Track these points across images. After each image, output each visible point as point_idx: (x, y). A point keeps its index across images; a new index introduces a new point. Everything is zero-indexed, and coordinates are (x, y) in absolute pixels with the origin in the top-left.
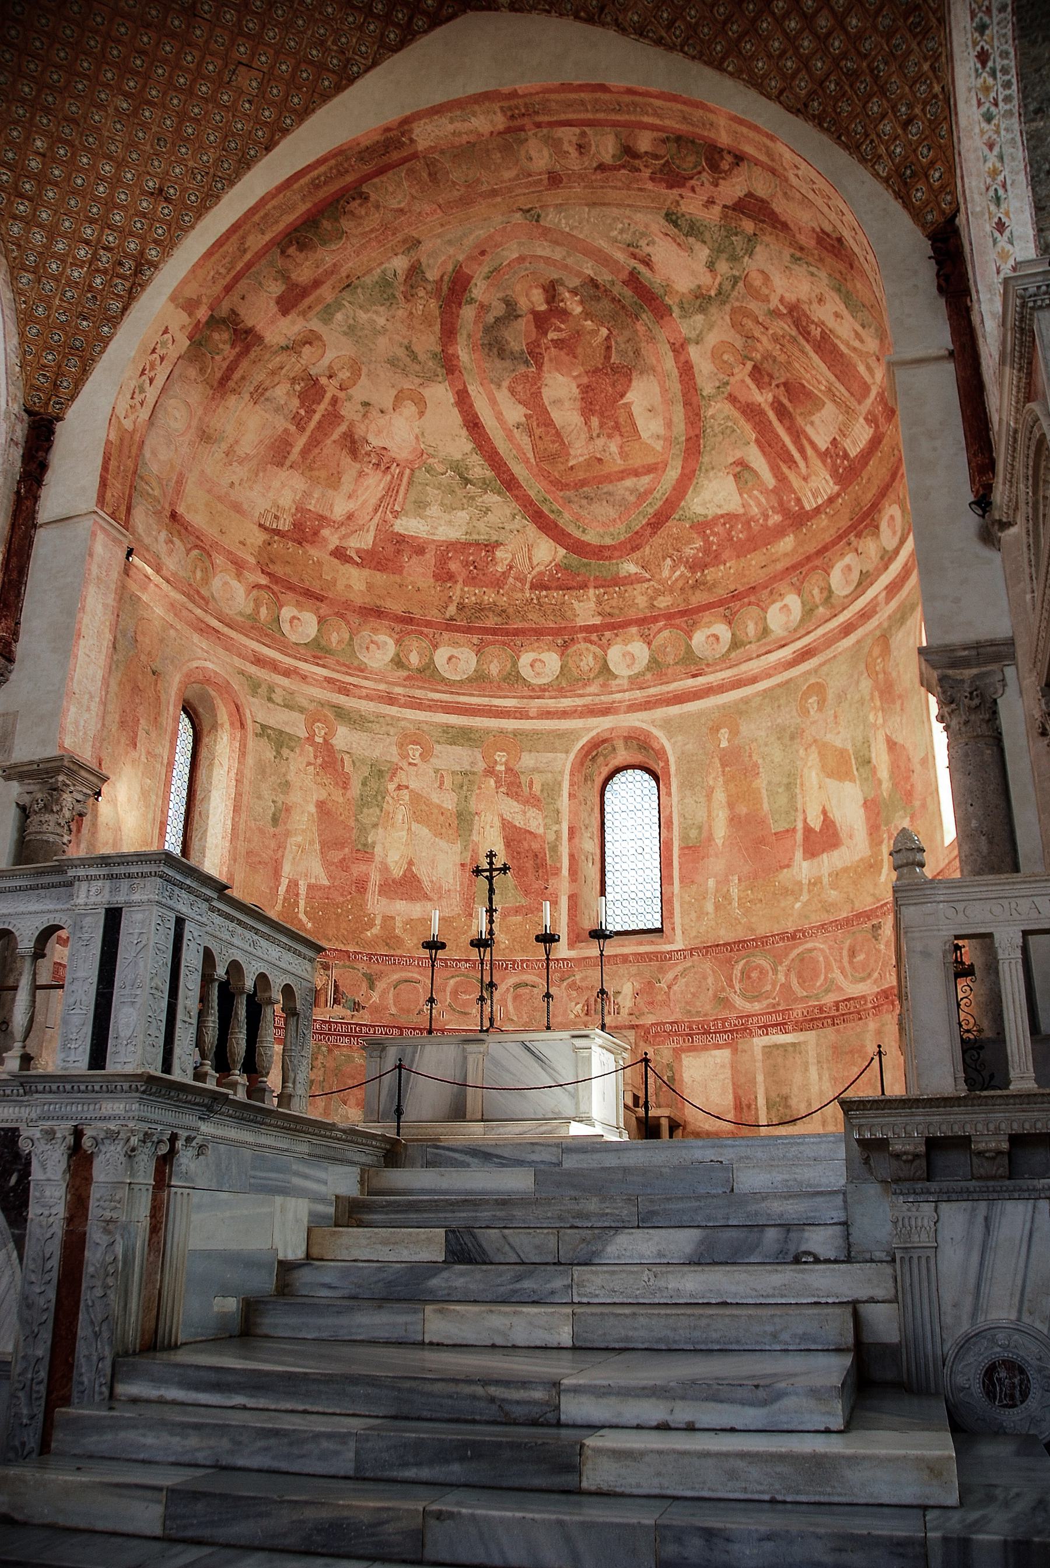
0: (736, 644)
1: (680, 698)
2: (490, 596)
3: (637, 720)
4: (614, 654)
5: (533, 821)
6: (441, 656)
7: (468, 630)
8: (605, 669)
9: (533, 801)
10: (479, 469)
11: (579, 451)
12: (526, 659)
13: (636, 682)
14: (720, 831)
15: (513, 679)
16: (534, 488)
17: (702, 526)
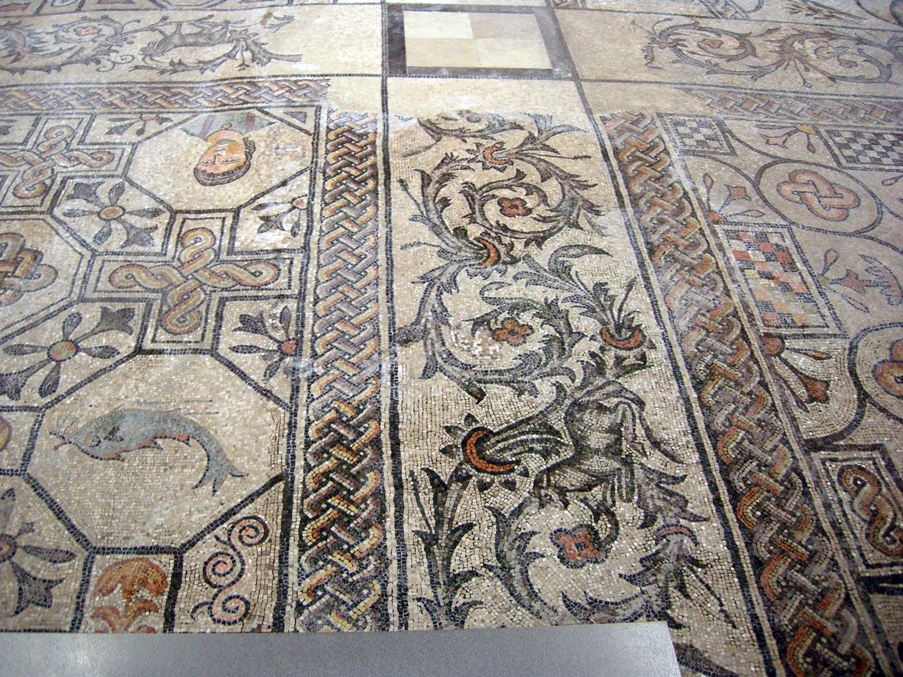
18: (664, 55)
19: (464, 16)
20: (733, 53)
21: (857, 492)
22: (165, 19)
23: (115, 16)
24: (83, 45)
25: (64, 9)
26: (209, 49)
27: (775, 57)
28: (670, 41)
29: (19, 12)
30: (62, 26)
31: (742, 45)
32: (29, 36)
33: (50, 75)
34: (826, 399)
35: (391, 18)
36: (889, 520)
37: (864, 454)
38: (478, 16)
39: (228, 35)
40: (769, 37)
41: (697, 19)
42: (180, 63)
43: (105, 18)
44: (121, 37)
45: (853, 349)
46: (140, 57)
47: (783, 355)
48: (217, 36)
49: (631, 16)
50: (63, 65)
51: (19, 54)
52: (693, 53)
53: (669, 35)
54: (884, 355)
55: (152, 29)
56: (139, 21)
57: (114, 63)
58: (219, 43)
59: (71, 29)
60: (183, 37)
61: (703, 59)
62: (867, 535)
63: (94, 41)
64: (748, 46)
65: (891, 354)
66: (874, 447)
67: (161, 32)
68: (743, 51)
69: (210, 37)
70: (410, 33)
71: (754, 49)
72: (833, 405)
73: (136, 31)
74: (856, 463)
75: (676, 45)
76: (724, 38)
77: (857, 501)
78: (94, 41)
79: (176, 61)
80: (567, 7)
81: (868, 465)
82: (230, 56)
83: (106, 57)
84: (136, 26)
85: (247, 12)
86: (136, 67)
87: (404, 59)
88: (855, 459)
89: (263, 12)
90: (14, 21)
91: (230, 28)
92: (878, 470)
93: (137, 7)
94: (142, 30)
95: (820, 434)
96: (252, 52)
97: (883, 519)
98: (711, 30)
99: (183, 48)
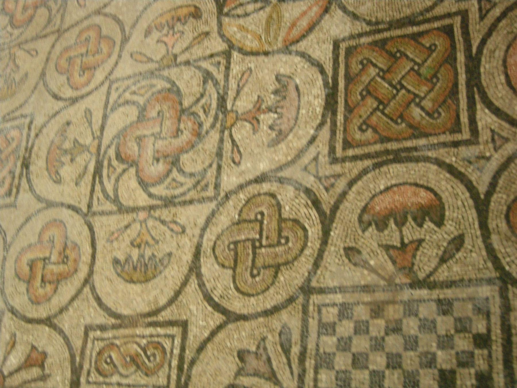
21: (115, 366)
34: (45, 355)
36: (139, 350)
37: (89, 345)
45: (13, 311)
47: (6, 373)
54: (22, 287)
62: (147, 375)
65: (24, 281)
66: (86, 334)
72: (50, 350)
74: (94, 354)
77: (121, 370)
81: (98, 345)
88: (91, 355)
92: (103, 339)
95: (68, 374)
97: (138, 355)
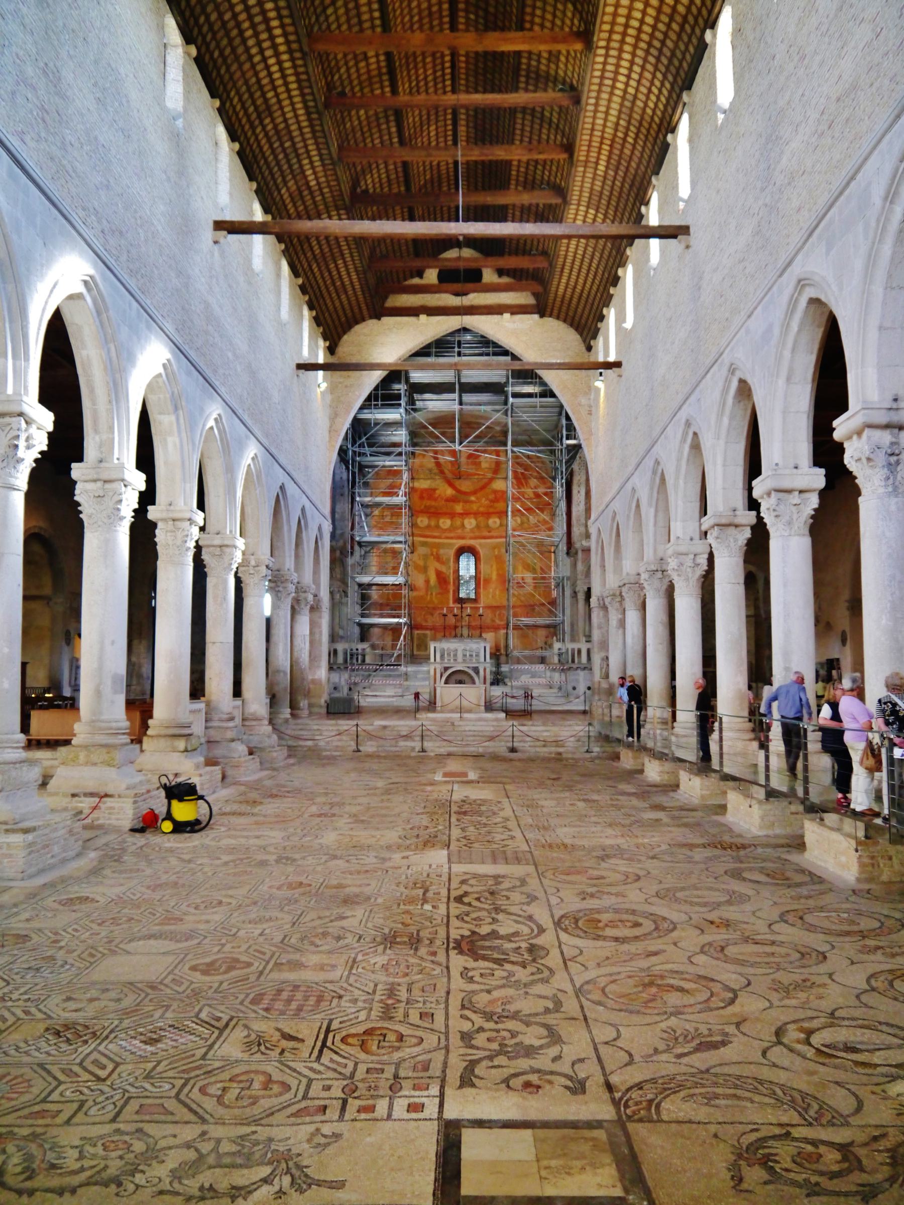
0: (501, 525)
1: (484, 538)
2: (433, 503)
3: (472, 542)
4: (466, 522)
5: (443, 569)
6: (419, 520)
7: (427, 513)
8: (463, 526)
9: (443, 563)
10: (435, 470)
11: (463, 468)
12: (441, 521)
13: (472, 530)
14: (494, 576)
15: (437, 527)
16: (450, 476)
17: (495, 492)
18: (754, 1175)
19: (527, 1133)
20: (835, 1168)
22: (204, 1133)
23: (149, 1128)
24: (110, 1163)
25: (97, 1119)
26: (245, 1171)
27: (886, 1171)
28: (759, 1156)
29: (48, 1121)
30: (90, 1139)
31: (845, 1159)
32: (50, 1149)
33: (61, 1200)
35: (447, 1136)
38: (541, 1133)
39: (269, 1155)
40: (875, 1146)
41: (789, 1128)
42: (211, 1188)
43: (139, 1130)
44: (153, 1155)
46: (168, 1180)
48: (257, 1156)
49: (713, 1128)
50: (80, 1186)
51: (33, 1170)
52: (787, 1170)
53: (758, 1149)
55: (188, 1146)
56: (175, 1136)
57: (137, 1186)
58: (258, 1165)
59: (99, 1144)
60: (219, 1156)
61: (800, 1178)
63: (121, 1157)
64: (851, 1158)
67: (197, 1150)
68: (846, 1165)
69: (249, 1156)
70: (467, 1153)
71: (859, 1161)
73: (170, 1148)
75: (766, 1162)
76: (822, 1149)
78: (121, 1157)
79: (207, 1185)
80: (641, 1120)
82: (266, 1181)
83: (130, 1178)
84: (171, 1141)
85: (295, 1128)
86: (161, 1193)
87: (459, 1186)
89: (311, 1128)
90: (39, 1130)
91: (273, 1147)
93: (177, 1118)
94: (177, 1147)
96: (292, 1176)
98: (806, 1140)
99: (217, 1170)
